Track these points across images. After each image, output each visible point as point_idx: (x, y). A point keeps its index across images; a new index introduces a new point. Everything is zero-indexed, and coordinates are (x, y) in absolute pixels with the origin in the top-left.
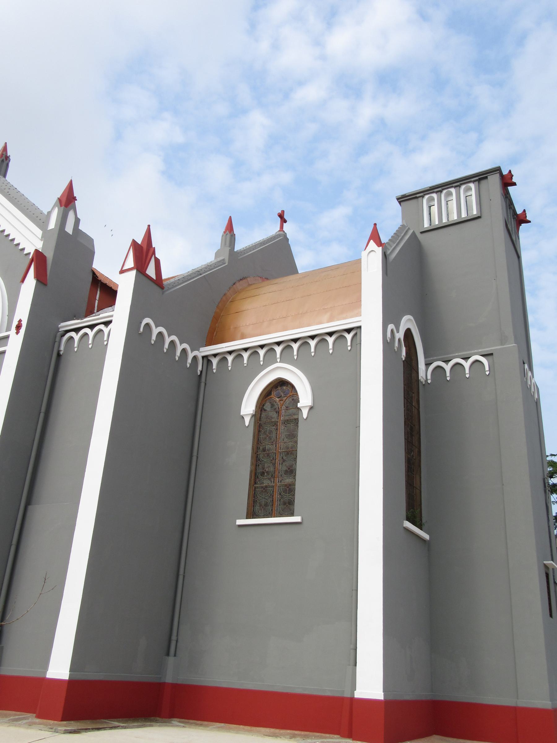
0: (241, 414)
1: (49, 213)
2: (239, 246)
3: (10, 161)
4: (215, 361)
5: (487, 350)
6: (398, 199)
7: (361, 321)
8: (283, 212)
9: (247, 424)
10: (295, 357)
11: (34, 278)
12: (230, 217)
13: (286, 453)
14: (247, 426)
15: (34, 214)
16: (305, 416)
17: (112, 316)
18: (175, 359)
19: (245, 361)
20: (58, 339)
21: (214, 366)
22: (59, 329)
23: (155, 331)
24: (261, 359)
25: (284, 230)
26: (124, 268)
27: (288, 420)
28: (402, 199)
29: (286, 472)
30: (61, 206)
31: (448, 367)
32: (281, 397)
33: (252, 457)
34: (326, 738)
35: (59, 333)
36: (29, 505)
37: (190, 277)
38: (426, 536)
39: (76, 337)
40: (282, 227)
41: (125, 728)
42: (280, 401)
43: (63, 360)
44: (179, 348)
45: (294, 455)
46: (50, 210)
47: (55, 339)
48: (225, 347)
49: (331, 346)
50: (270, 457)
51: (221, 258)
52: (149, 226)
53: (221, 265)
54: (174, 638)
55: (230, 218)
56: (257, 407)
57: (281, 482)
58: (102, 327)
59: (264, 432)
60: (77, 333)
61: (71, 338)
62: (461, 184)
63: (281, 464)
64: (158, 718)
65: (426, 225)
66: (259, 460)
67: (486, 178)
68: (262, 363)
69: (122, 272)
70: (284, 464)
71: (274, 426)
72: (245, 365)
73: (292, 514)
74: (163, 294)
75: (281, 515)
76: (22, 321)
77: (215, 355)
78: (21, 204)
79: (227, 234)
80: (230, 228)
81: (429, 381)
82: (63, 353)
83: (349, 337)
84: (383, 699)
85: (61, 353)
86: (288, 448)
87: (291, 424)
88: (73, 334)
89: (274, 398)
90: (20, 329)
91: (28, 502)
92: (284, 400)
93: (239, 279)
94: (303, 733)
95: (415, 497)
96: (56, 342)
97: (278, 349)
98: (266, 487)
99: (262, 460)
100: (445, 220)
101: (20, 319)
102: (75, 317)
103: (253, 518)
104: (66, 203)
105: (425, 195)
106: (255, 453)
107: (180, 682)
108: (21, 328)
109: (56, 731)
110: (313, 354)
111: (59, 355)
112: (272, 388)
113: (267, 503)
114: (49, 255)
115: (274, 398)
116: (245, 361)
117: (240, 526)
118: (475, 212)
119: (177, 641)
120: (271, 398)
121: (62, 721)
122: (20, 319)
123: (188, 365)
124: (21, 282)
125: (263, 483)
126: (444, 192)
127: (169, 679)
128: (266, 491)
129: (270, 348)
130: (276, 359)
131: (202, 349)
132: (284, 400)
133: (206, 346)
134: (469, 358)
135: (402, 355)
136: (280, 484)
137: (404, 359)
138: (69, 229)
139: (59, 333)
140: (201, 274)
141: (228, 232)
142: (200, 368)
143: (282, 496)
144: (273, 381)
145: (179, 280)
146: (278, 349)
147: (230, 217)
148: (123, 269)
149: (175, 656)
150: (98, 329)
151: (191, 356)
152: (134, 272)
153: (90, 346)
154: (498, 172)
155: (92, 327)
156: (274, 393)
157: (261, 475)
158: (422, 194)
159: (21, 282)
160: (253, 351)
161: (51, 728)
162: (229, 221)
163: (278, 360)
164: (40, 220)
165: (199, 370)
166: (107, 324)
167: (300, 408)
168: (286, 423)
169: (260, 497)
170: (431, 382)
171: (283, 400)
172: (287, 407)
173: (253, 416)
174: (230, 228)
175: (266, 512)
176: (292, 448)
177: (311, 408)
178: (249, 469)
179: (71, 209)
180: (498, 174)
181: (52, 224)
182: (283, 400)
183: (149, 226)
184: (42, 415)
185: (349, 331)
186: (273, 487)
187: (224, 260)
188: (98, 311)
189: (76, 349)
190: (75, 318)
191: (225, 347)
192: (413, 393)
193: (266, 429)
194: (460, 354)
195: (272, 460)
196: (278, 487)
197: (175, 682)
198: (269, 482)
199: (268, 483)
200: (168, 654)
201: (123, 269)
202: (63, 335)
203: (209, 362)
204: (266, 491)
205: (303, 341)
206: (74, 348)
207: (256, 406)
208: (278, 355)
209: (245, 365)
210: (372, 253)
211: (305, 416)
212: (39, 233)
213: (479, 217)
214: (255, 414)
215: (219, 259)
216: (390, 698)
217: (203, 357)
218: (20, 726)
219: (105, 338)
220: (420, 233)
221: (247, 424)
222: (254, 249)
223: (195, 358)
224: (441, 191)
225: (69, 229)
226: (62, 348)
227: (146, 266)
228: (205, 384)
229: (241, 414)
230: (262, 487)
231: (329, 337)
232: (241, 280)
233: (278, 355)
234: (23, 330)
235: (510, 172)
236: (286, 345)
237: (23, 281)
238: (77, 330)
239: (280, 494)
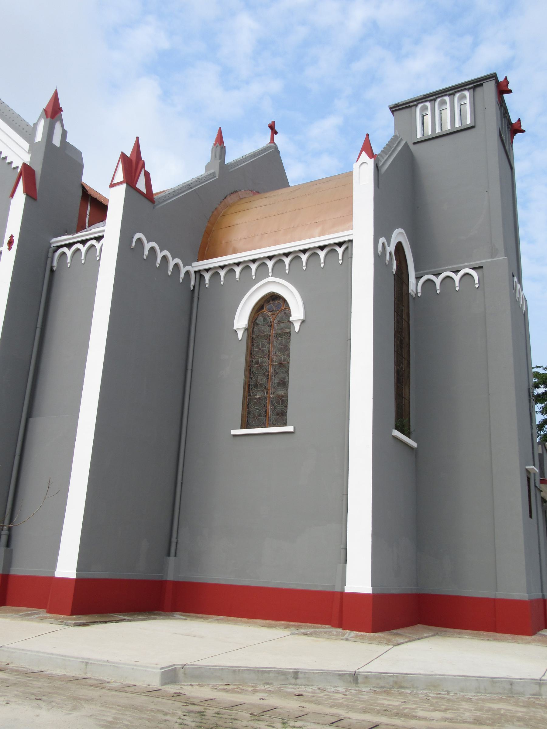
0: (234, 328)
1: (36, 125)
2: (229, 159)
4: (207, 276)
5: (477, 263)
6: (391, 108)
7: (352, 234)
8: (274, 122)
9: (240, 337)
10: (287, 272)
11: (24, 193)
12: (220, 128)
13: (278, 366)
14: (240, 339)
15: (19, 126)
16: (297, 329)
17: (103, 231)
18: (168, 274)
19: (238, 276)
20: (50, 255)
21: (207, 281)
22: (51, 244)
23: (148, 246)
24: (253, 273)
26: (114, 182)
27: (280, 334)
28: (395, 109)
29: (279, 384)
30: (47, 117)
31: (438, 281)
32: (274, 311)
33: (246, 370)
34: (318, 628)
35: (51, 250)
36: (30, 417)
37: (180, 191)
38: (414, 444)
39: (69, 252)
40: (272, 138)
41: (131, 621)
42: (272, 314)
43: (57, 276)
44: (172, 263)
45: (286, 368)
46: (36, 122)
47: (48, 256)
48: (218, 262)
49: (322, 260)
50: (263, 370)
51: (212, 171)
52: (138, 138)
53: (212, 178)
54: (174, 539)
55: (220, 129)
56: (250, 322)
57: (274, 393)
58: (94, 242)
59: (257, 346)
60: (69, 249)
61: (64, 254)
62: (456, 92)
63: (274, 376)
64: (161, 612)
65: (419, 135)
66: (252, 373)
68: (254, 277)
69: (112, 186)
70: (276, 376)
71: (266, 340)
72: (237, 280)
73: (285, 424)
74: (154, 208)
75: (274, 424)
76: (13, 237)
77: (207, 270)
78: (6, 116)
79: (217, 146)
80: (220, 140)
81: (419, 295)
82: (56, 269)
83: (340, 250)
84: (371, 593)
85: (55, 269)
86: (281, 361)
87: (283, 338)
88: (65, 250)
89: (266, 312)
90: (12, 245)
91: (29, 415)
92: (276, 314)
93: (230, 193)
94: (296, 624)
95: (404, 408)
96: (48, 257)
97: (270, 264)
98: (260, 398)
99: (255, 373)
100: (438, 130)
101: (12, 235)
102: (67, 232)
103: (247, 428)
104: (52, 112)
105: (418, 103)
106: (249, 366)
107: (180, 580)
108: (13, 244)
109: (66, 624)
110: (304, 268)
111: (52, 271)
112: (264, 302)
113: (261, 413)
114: (38, 169)
115: (266, 312)
116: (238, 276)
117: (235, 436)
118: (469, 121)
119: (177, 543)
120: (263, 312)
121: (71, 615)
122: (12, 235)
123: (181, 281)
124: (10, 197)
125: (257, 394)
126: (438, 100)
127: (171, 577)
128: (259, 403)
129: (261, 262)
130: (268, 273)
131: (194, 264)
132: (276, 314)
133: (198, 260)
134: (459, 271)
135: (393, 268)
136: (273, 396)
137: (395, 273)
138: (57, 141)
139: (51, 249)
140: (191, 188)
141: (218, 144)
142: (193, 283)
143: (275, 407)
144: (265, 295)
145: (169, 194)
146: (270, 264)
147: (220, 128)
148: (113, 183)
149: (175, 556)
150: (90, 245)
151: (183, 271)
152: (124, 186)
153: (83, 262)
154: (494, 78)
155: (83, 242)
156: (266, 308)
157: (255, 388)
158: (415, 103)
159: (10, 197)
160: (245, 266)
161: (62, 622)
162: (218, 132)
163: (270, 274)
164: (26, 132)
165: (192, 285)
166: (99, 239)
167: (292, 322)
168: (278, 336)
169: (254, 408)
170: (421, 296)
171: (275, 314)
172: (279, 321)
173: (246, 330)
174: (220, 140)
175: (260, 422)
176: (284, 360)
177: (303, 322)
178: (243, 381)
179: (58, 121)
180: (494, 81)
181: (39, 137)
182: (275, 314)
183: (138, 138)
184: (38, 331)
185: (340, 244)
186: (266, 398)
187: (214, 173)
188: (89, 226)
189: (69, 265)
190: (66, 234)
191: (218, 262)
192: (403, 306)
193: (259, 342)
194: (450, 267)
195: (264, 373)
196: (272, 398)
197: (176, 580)
198: (262, 394)
199: (262, 395)
200: (169, 555)
201: (113, 183)
202: (55, 251)
203: (202, 277)
204: (259, 403)
205: (295, 256)
206: (67, 263)
207: (249, 321)
208: (270, 270)
209: (237, 280)
210: (365, 164)
211: (297, 329)
212: (26, 145)
213: (473, 127)
214: (248, 328)
215: (209, 172)
216: (378, 592)
217: (196, 272)
218: (32, 621)
219: (98, 254)
220: (412, 144)
221: (240, 338)
222: (244, 162)
223: (187, 273)
224: (435, 100)
225: (57, 141)
226: (55, 264)
227: (136, 178)
228: (198, 299)
229: (234, 328)
230: (256, 399)
231: (320, 251)
232: (232, 193)
233: (270, 270)
234: (15, 246)
235: (506, 78)
236: (278, 259)
237: (12, 195)
238: (69, 246)
239: (273, 405)
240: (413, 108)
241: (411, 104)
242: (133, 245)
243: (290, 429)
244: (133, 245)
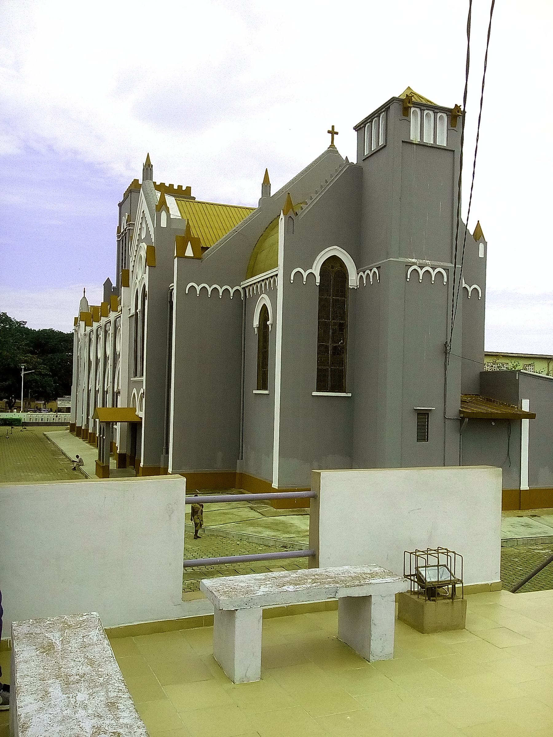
2: (273, 192)
3: (152, 166)
6: (354, 129)
8: (333, 127)
23: (198, 289)
25: (335, 144)
31: (364, 277)
38: (350, 395)
62: (380, 114)
67: (389, 107)
81: (358, 287)
117: (256, 394)
137: (318, 284)
138: (164, 224)
140: (237, 231)
149: (242, 459)
158: (363, 125)
217: (243, 288)
240: (363, 128)
241: (361, 126)
242: (187, 292)
243: (266, 392)
244: (187, 292)
